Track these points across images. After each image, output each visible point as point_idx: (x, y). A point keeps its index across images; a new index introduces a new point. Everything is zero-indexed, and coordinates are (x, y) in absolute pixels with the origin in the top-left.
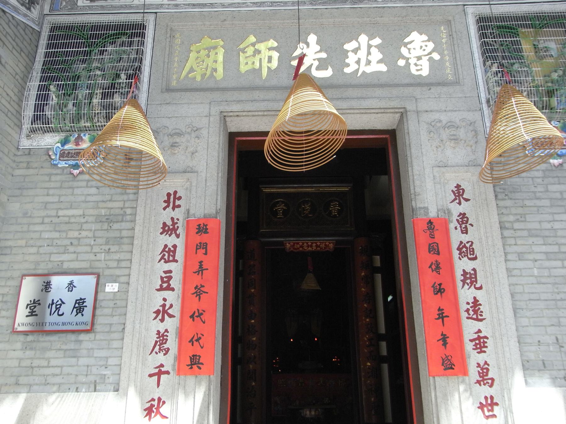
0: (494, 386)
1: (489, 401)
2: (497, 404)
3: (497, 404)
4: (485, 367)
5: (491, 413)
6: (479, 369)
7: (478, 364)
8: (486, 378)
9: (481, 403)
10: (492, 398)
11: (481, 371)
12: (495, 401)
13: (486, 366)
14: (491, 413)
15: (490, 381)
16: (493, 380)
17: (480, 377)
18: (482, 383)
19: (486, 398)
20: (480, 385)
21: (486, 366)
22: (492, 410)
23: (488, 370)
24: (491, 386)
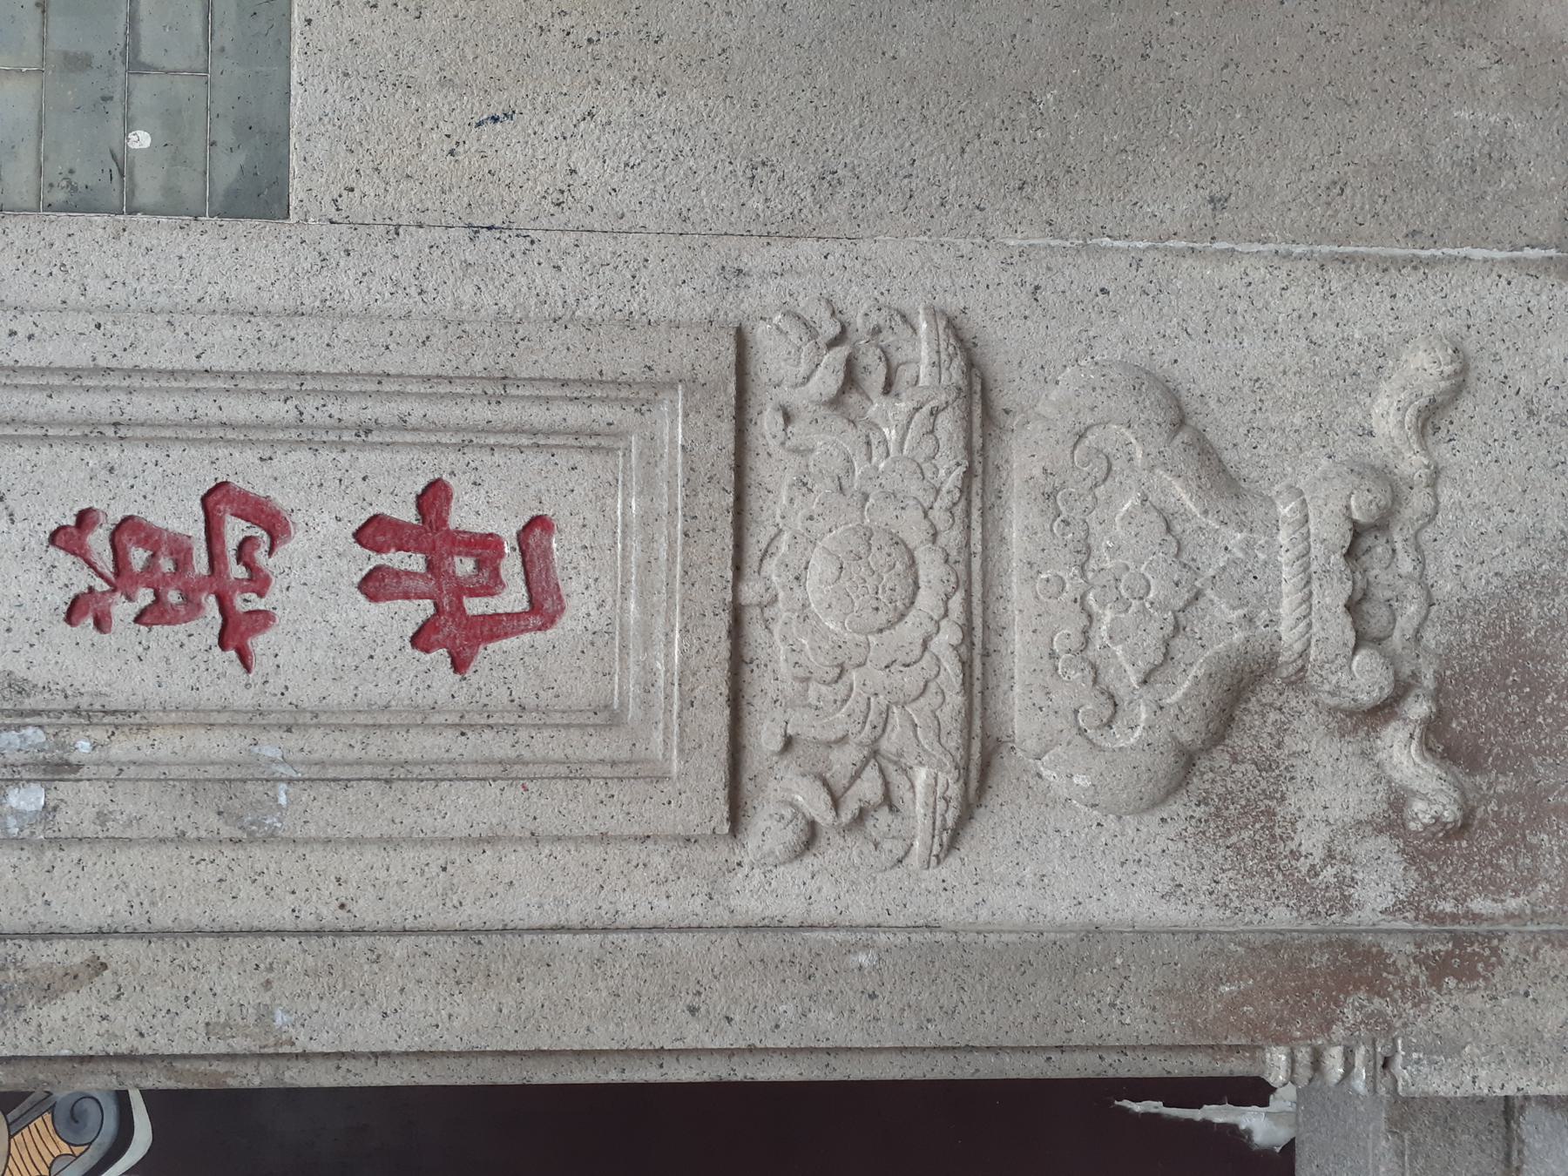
0: (282, 499)
1: (415, 562)
2: (434, 497)
3: (434, 497)
4: (105, 561)
5: (511, 566)
6: (123, 610)
7: (73, 612)
8: (200, 563)
9: (422, 639)
10: (374, 532)
11: (145, 597)
12: (408, 514)
13: (98, 541)
14: (511, 566)
15: (235, 530)
16: (216, 500)
17: (192, 608)
18: (244, 603)
19: (374, 586)
20: (263, 619)
21: (98, 541)
22: (485, 548)
23: (128, 529)
24: (275, 525)
